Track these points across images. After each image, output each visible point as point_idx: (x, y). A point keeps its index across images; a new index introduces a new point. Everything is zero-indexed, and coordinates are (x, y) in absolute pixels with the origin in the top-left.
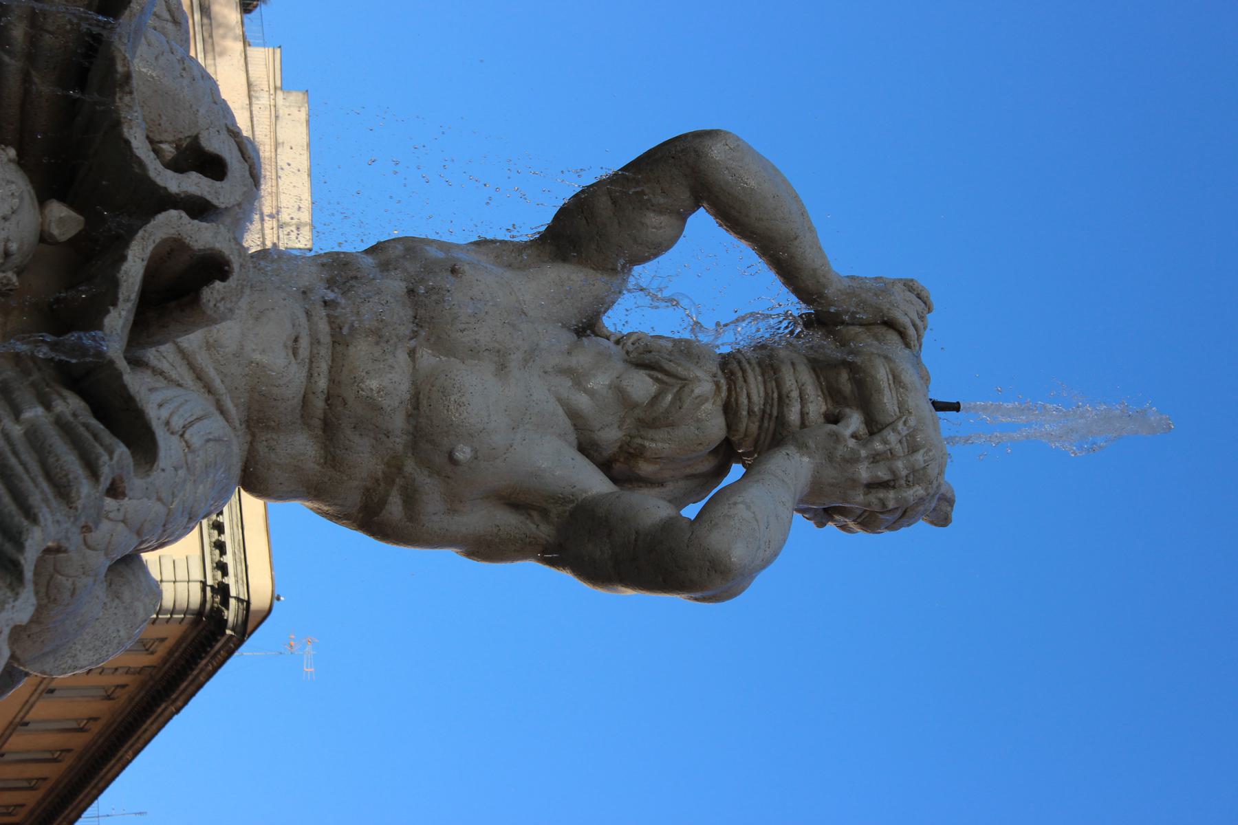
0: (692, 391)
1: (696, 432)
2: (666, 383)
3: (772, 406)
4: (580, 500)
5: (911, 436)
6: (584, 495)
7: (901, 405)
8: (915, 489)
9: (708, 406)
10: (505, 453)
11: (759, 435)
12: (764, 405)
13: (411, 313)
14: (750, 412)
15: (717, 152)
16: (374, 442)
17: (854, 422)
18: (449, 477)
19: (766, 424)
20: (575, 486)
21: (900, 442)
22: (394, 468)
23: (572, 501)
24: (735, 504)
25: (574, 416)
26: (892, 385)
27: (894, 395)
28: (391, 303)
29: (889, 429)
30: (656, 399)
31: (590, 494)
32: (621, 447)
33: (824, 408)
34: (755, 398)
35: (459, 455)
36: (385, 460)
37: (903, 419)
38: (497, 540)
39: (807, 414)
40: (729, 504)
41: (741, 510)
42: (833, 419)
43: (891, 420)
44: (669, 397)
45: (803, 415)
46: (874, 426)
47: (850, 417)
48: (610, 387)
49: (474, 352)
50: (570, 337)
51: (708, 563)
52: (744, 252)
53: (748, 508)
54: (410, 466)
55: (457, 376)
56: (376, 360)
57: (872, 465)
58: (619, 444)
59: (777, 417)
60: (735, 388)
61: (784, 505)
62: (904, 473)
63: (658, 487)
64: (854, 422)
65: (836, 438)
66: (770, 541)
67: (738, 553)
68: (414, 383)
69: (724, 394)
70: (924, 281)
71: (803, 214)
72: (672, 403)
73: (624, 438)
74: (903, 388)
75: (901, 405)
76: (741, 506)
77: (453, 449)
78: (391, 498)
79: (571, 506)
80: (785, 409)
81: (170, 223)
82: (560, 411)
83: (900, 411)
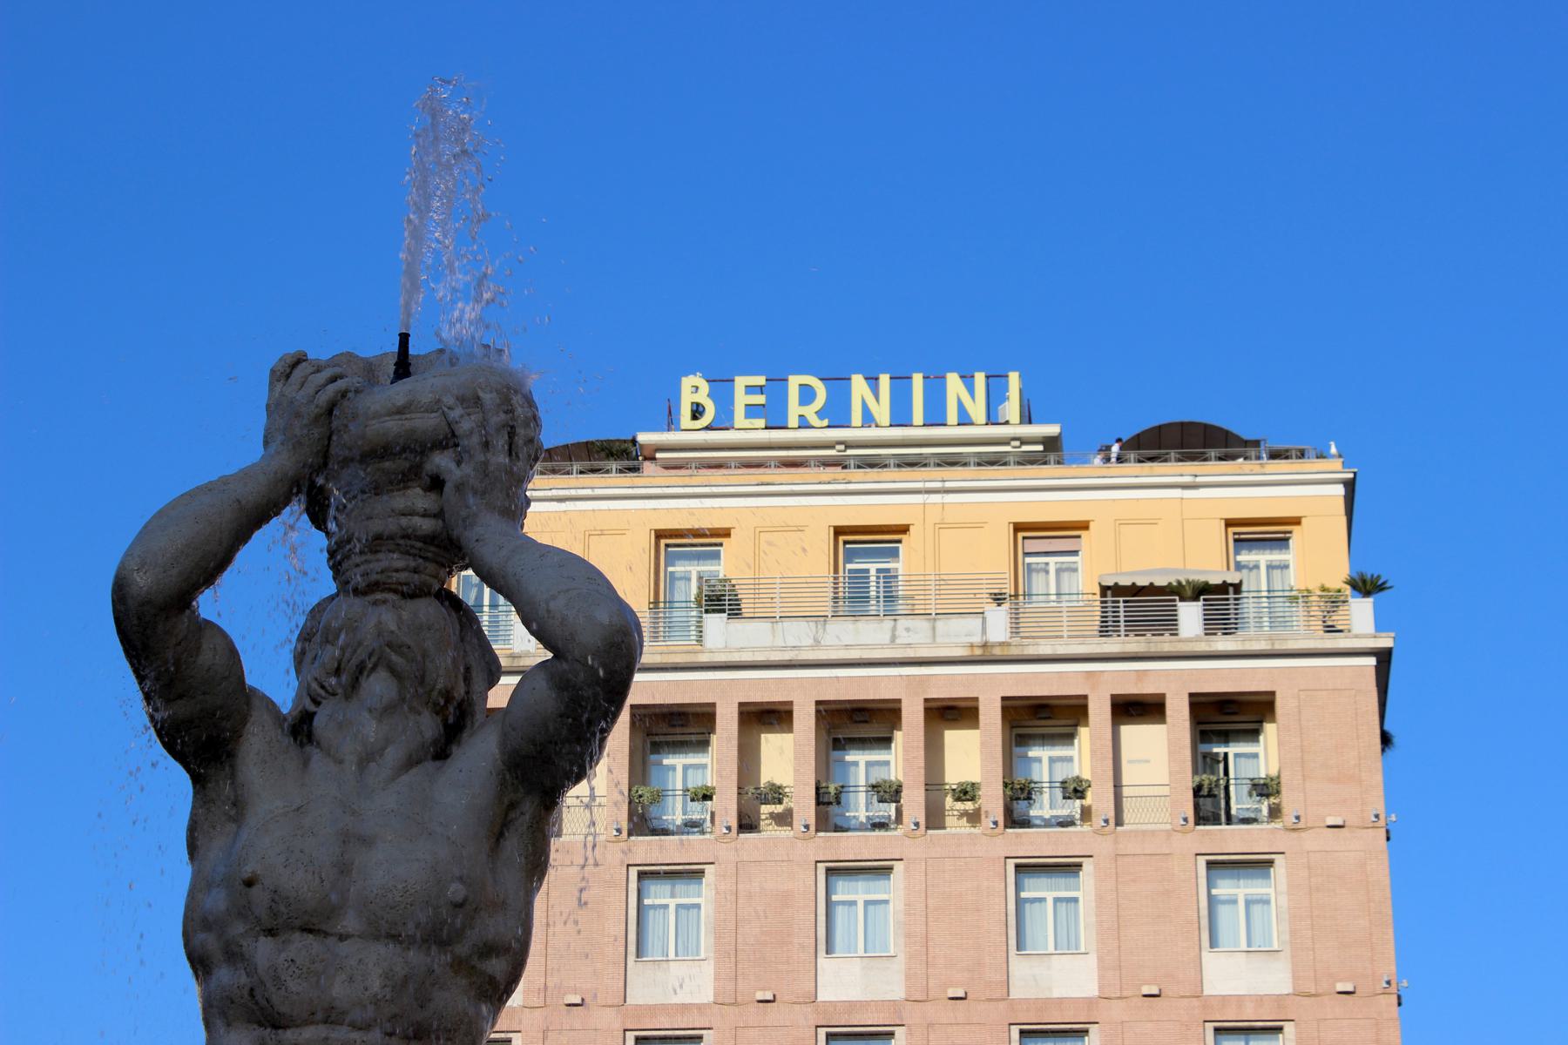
0: (392, 632)
1: (432, 631)
2: (379, 659)
3: (412, 547)
4: (503, 768)
5: (462, 400)
6: (499, 762)
7: (430, 410)
8: (517, 406)
9: (405, 615)
10: (457, 846)
11: (437, 562)
12: (410, 555)
13: (297, 935)
14: (415, 571)
15: (142, 582)
16: (437, 986)
17: (442, 461)
18: (476, 909)
19: (429, 555)
20: (491, 772)
21: (469, 415)
22: (460, 966)
23: (504, 775)
24: (548, 611)
25: (411, 763)
26: (408, 416)
27: (419, 415)
28: (288, 956)
29: (455, 427)
30: (393, 671)
31: (498, 757)
32: (437, 714)
33: (419, 491)
34: (400, 564)
35: (459, 898)
36: (453, 974)
37: (446, 409)
38: (532, 858)
39: (425, 510)
40: (548, 617)
41: (558, 605)
42: (436, 484)
43: (444, 423)
44: (394, 657)
45: (425, 514)
47: (438, 467)
48: (380, 721)
49: (344, 869)
50: (316, 756)
51: (613, 649)
52: (243, 556)
53: (554, 598)
54: (462, 949)
55: (372, 891)
56: (351, 979)
57: (491, 449)
58: (434, 715)
59: (425, 543)
60: (389, 584)
61: (543, 555)
62: (503, 416)
63: (470, 673)
64: (442, 461)
65: (459, 488)
66: (588, 578)
67: (603, 616)
68: (377, 938)
69: (391, 596)
70: (272, 356)
71: (208, 488)
72: (402, 654)
73: (430, 709)
74: (411, 405)
75: (430, 410)
76: (552, 605)
77: (451, 902)
78: (488, 970)
79: (508, 777)
80: (419, 533)
82: (405, 778)
83: (436, 412)
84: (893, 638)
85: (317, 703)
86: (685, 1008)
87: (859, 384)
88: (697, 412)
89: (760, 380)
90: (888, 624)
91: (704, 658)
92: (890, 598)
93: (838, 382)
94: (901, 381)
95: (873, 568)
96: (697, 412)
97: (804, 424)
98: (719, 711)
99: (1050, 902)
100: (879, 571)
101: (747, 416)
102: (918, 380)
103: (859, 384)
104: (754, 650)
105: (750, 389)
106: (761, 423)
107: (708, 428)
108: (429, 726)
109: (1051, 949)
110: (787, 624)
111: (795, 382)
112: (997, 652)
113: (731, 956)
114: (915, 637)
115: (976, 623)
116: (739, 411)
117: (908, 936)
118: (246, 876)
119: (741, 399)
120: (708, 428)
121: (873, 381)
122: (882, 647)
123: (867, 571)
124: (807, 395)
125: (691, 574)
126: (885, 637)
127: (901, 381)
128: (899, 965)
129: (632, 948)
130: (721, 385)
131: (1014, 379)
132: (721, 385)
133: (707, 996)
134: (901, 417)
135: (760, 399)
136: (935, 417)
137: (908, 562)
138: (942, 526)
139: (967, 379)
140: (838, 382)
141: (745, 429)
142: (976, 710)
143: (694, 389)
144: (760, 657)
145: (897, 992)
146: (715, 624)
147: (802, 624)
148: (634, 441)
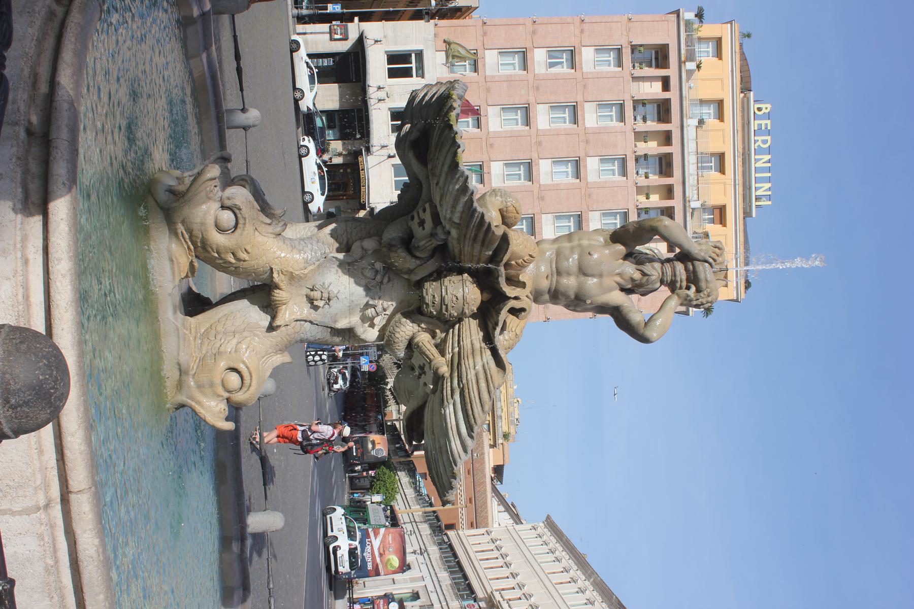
17: (693, 288)
25: (618, 284)
42: (688, 288)
46: (698, 291)
81: (512, 304)
84: (691, 175)
85: (634, 258)
86: (584, 119)
87: (767, 157)
88: (759, 109)
89: (769, 128)
90: (696, 173)
91: (685, 120)
92: (703, 168)
93: (769, 151)
94: (769, 170)
95: (713, 164)
96: (759, 109)
97: (755, 142)
98: (669, 124)
99: (615, 221)
100: (712, 166)
101: (758, 124)
102: (769, 175)
103: (767, 157)
104: (687, 134)
105: (766, 125)
106: (756, 129)
107: (754, 112)
108: (629, 286)
109: (603, 222)
110: (695, 143)
111: (769, 138)
112: (687, 204)
113: (599, 132)
114: (691, 180)
115: (695, 197)
116: (760, 122)
117: (606, 182)
118: (591, 253)
119: (763, 122)
120: (754, 112)
121: (769, 161)
122: (689, 171)
123: (711, 163)
124: (765, 142)
125: (709, 112)
126: (691, 172)
127: (769, 170)
128: (597, 180)
129: (600, 103)
130: (768, 116)
131: (769, 203)
132: (768, 116)
133: (588, 125)
134: (757, 170)
135: (763, 128)
136: (757, 180)
137: (714, 174)
138: (725, 184)
139: (769, 189)
140: (769, 151)
141: (754, 125)
142: (671, 199)
143: (766, 107)
144: (685, 136)
145: (590, 179)
146: (695, 122)
147: (695, 148)
148: (750, 90)
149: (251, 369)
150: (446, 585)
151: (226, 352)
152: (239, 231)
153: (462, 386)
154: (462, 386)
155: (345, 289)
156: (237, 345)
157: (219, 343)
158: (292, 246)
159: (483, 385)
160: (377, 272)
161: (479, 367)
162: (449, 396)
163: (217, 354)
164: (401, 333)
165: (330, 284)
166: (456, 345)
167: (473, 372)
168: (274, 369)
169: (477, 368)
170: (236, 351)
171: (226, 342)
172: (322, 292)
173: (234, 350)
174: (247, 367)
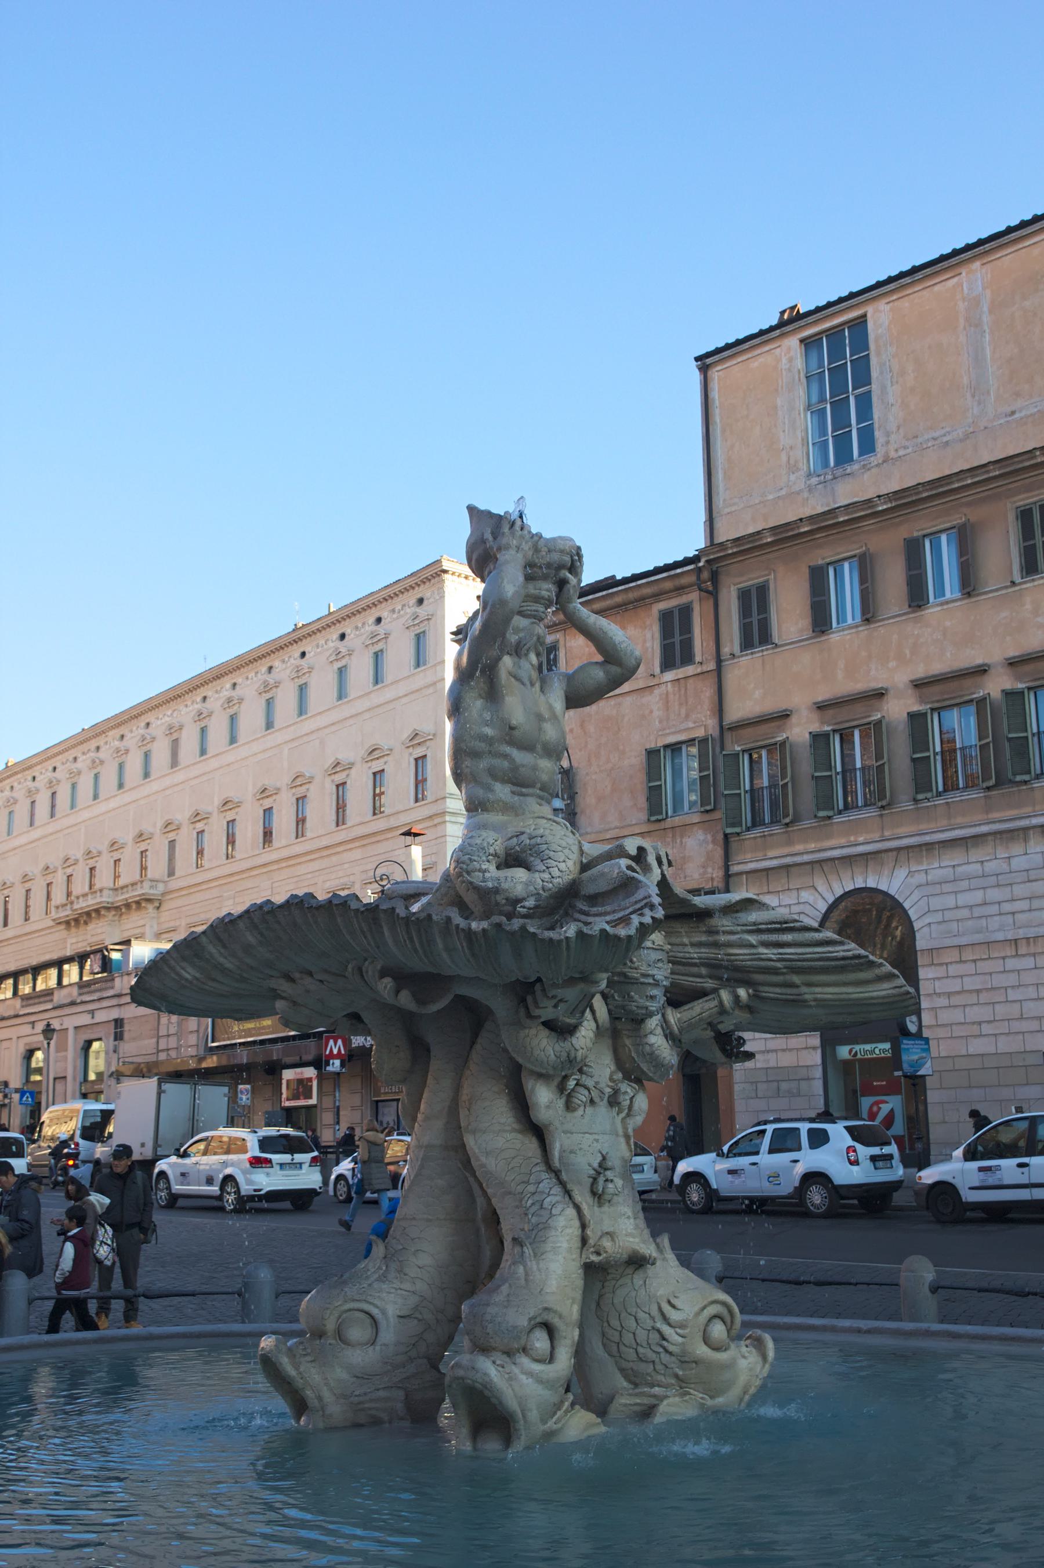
149: (705, 1302)
150: (80, 994)
151: (683, 1343)
152: (556, 1321)
153: (785, 970)
154: (785, 970)
155: (597, 1141)
156: (670, 1325)
157: (663, 1355)
158: (545, 1228)
159: (788, 937)
160: (577, 1084)
161: (752, 939)
162: (794, 991)
163: (683, 1359)
164: (665, 1055)
165: (590, 1165)
166: (695, 970)
167: (762, 950)
168: (682, 1266)
169: (754, 942)
170: (682, 1326)
171: (665, 1343)
172: (607, 1180)
173: (679, 1331)
174: (704, 1308)
